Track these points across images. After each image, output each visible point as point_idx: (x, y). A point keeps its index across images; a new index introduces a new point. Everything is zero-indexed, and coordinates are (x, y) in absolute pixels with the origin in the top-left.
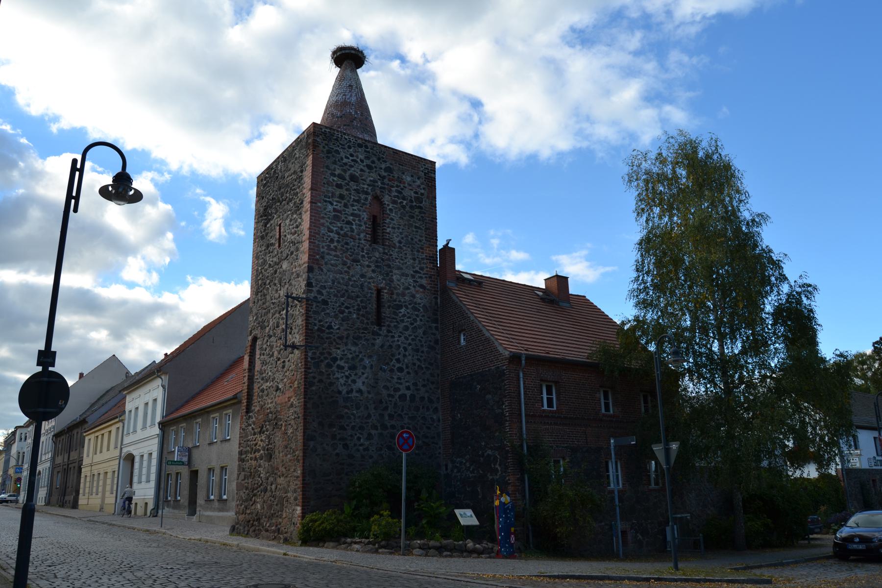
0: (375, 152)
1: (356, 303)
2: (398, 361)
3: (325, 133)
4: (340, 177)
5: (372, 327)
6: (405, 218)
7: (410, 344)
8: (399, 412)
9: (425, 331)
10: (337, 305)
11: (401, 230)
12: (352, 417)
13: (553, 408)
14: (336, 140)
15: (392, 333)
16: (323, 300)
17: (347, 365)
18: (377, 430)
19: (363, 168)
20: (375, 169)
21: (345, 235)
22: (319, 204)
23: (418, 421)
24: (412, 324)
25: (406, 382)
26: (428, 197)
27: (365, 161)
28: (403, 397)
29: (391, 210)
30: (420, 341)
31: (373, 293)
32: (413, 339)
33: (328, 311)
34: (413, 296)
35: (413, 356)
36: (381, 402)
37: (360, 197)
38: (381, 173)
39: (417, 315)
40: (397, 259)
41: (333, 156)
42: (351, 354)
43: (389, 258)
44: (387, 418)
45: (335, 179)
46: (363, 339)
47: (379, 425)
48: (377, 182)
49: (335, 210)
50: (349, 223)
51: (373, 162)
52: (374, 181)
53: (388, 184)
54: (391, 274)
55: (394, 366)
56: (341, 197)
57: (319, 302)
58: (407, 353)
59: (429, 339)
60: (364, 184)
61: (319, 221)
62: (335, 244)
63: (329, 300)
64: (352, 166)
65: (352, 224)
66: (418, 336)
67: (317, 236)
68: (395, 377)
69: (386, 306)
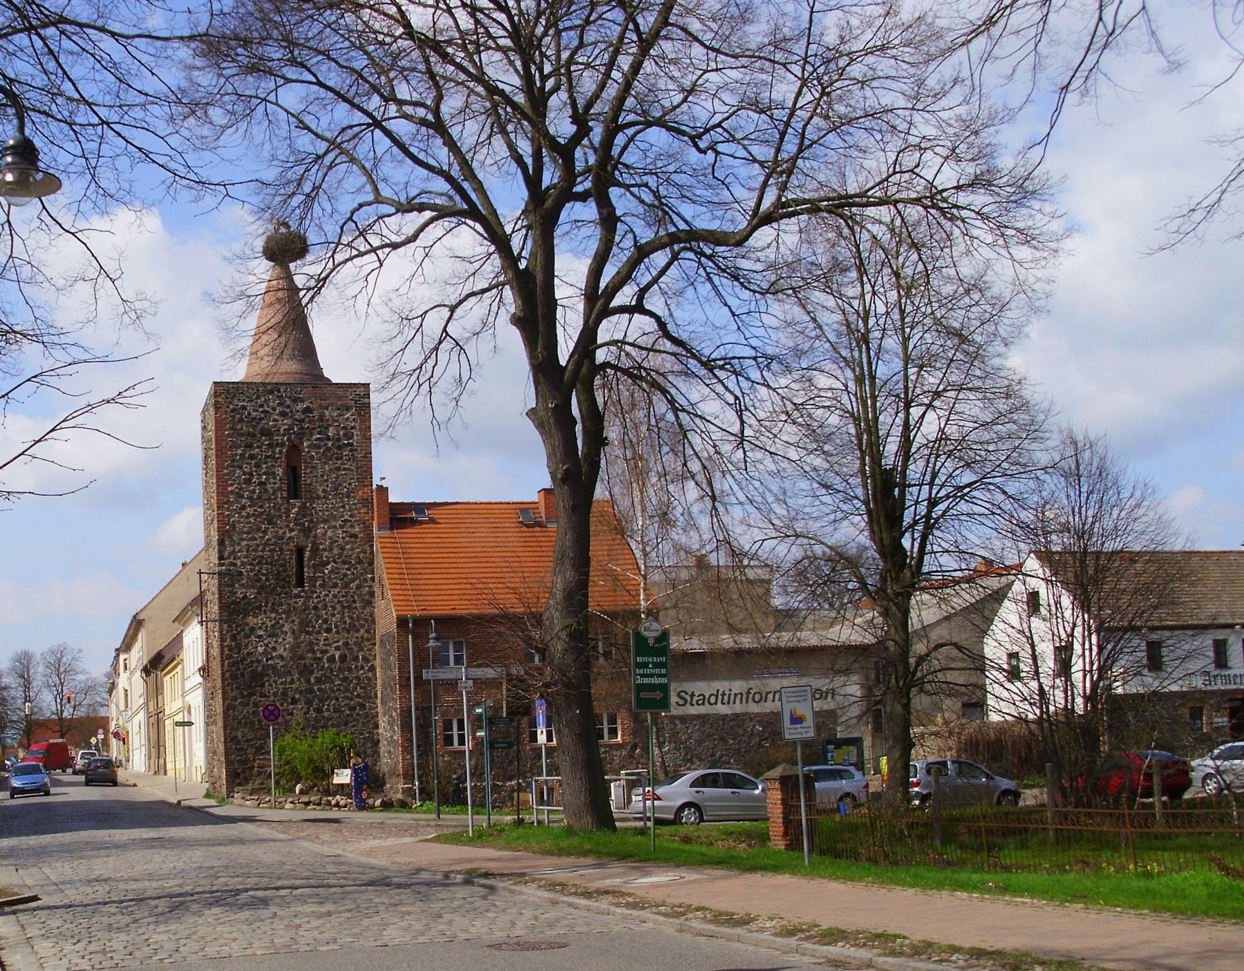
4: (249, 434)
19: (275, 417)
25: (335, 642)
38: (296, 417)
51: (288, 407)
56: (252, 457)
64: (262, 419)
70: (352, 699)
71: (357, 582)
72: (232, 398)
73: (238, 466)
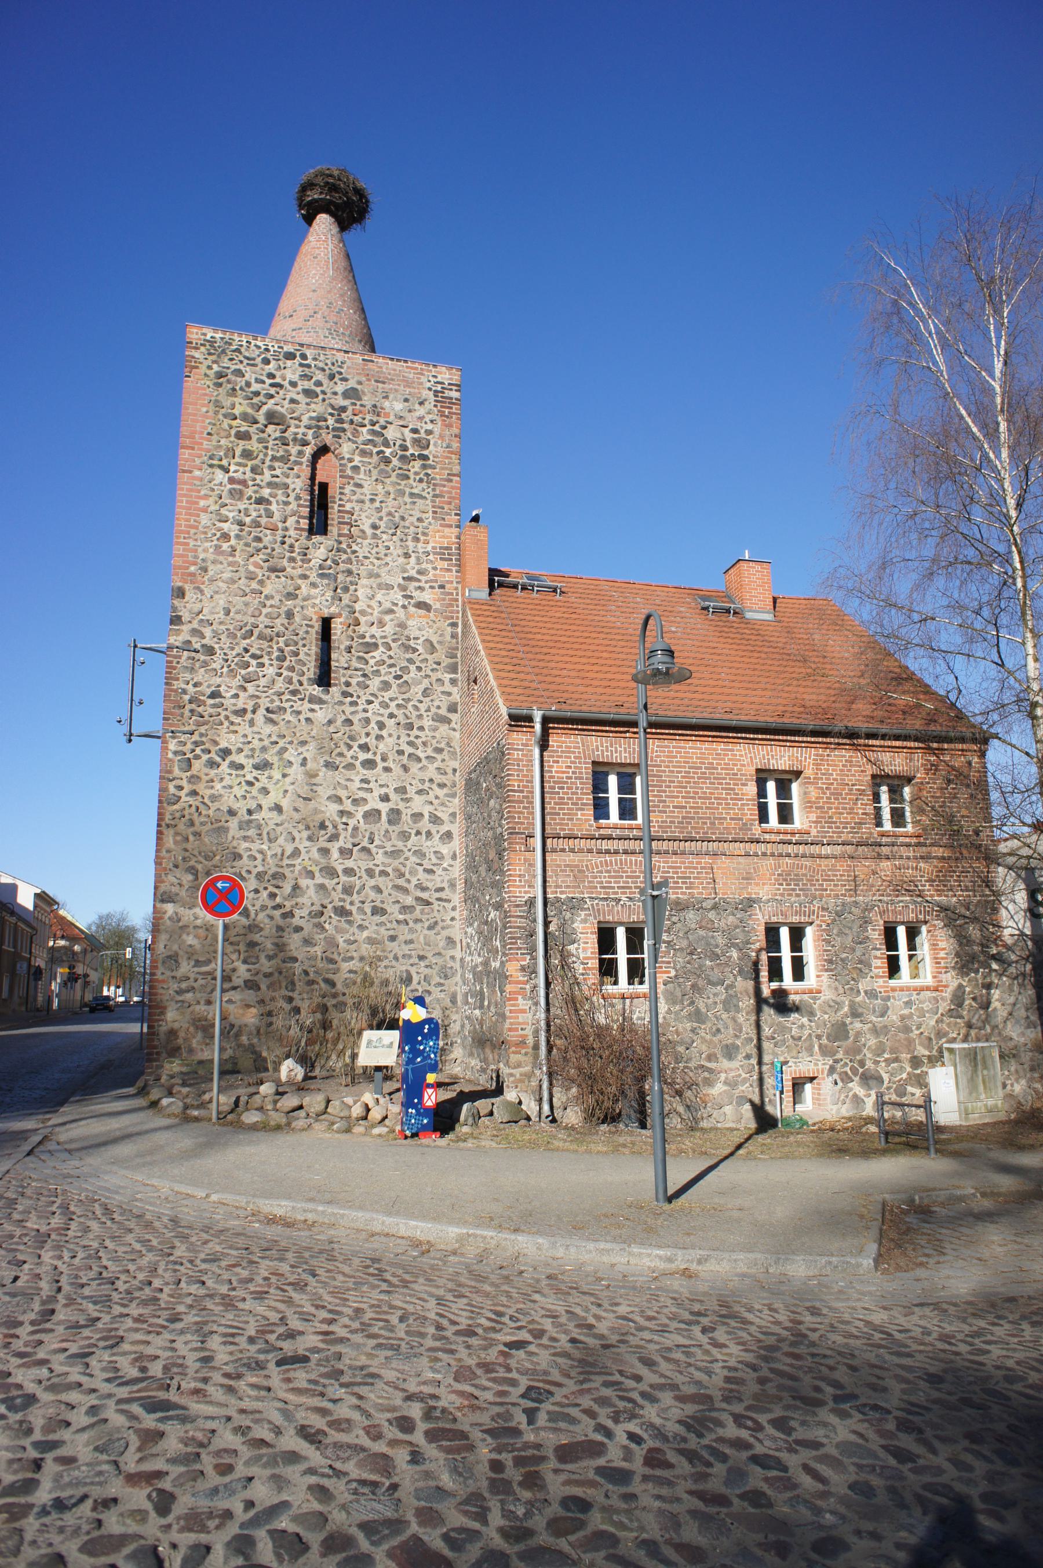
0: (321, 365)
1: (275, 647)
2: (365, 747)
3: (212, 342)
4: (245, 417)
5: (310, 688)
6: (388, 481)
7: (391, 716)
8: (365, 843)
9: (426, 689)
10: (234, 653)
11: (377, 504)
12: (259, 856)
13: (635, 818)
14: (238, 351)
15: (352, 696)
16: (203, 646)
17: (251, 761)
18: (313, 878)
20: (321, 397)
21: (257, 524)
22: (197, 473)
23: (407, 859)
24: (398, 677)
25: (381, 786)
26: (442, 437)
27: (300, 383)
28: (373, 815)
29: (356, 469)
30: (416, 708)
31: (312, 627)
32: (398, 706)
33: (214, 666)
34: (402, 626)
35: (399, 738)
36: (323, 826)
37: (287, 451)
38: (332, 401)
39: (411, 661)
40: (366, 558)
41: (229, 382)
42: (261, 740)
43: (350, 559)
44: (335, 854)
45: (235, 423)
46: (289, 711)
47: (315, 869)
48: (326, 420)
49: (231, 480)
50: (260, 501)
51: (319, 384)
52: (321, 419)
53: (352, 422)
54: (352, 588)
55: (357, 758)
56: (247, 454)
57: (196, 651)
58: (384, 733)
59: (436, 703)
60: (298, 427)
61: (197, 503)
62: (233, 542)
63: (216, 646)
65: (269, 503)
66: (409, 700)
67: (193, 531)
68: (357, 779)
69: (342, 647)
70: (406, 891)
71: (426, 683)
72: (219, 356)
73: (221, 467)
